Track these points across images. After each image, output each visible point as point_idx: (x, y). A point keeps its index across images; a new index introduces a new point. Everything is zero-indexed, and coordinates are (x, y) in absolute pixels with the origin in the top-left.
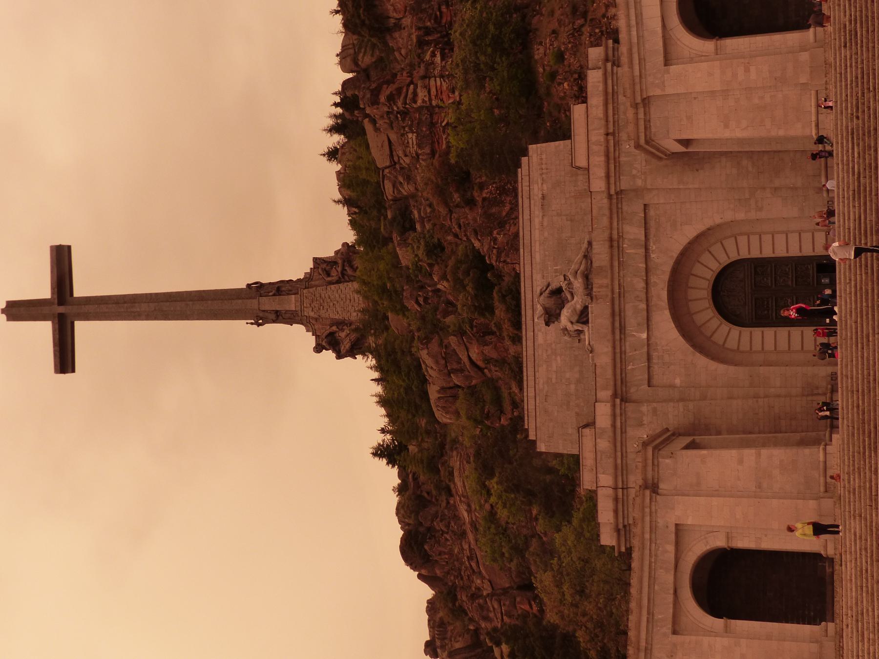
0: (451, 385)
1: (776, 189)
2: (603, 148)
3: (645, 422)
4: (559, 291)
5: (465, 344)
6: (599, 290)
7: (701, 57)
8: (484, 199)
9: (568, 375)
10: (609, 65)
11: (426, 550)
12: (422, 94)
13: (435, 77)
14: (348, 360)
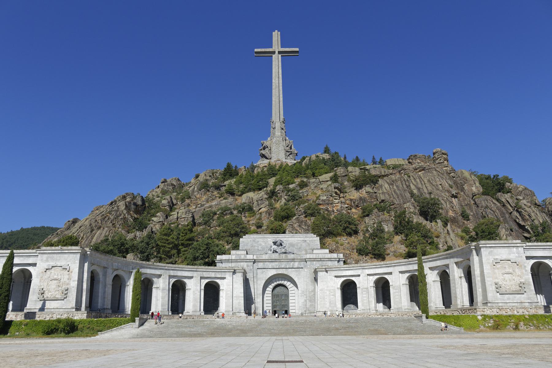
1: (306, 301)
2: (317, 258)
4: (281, 245)
8: (307, 221)
9: (260, 247)
10: (338, 259)
12: (337, 201)
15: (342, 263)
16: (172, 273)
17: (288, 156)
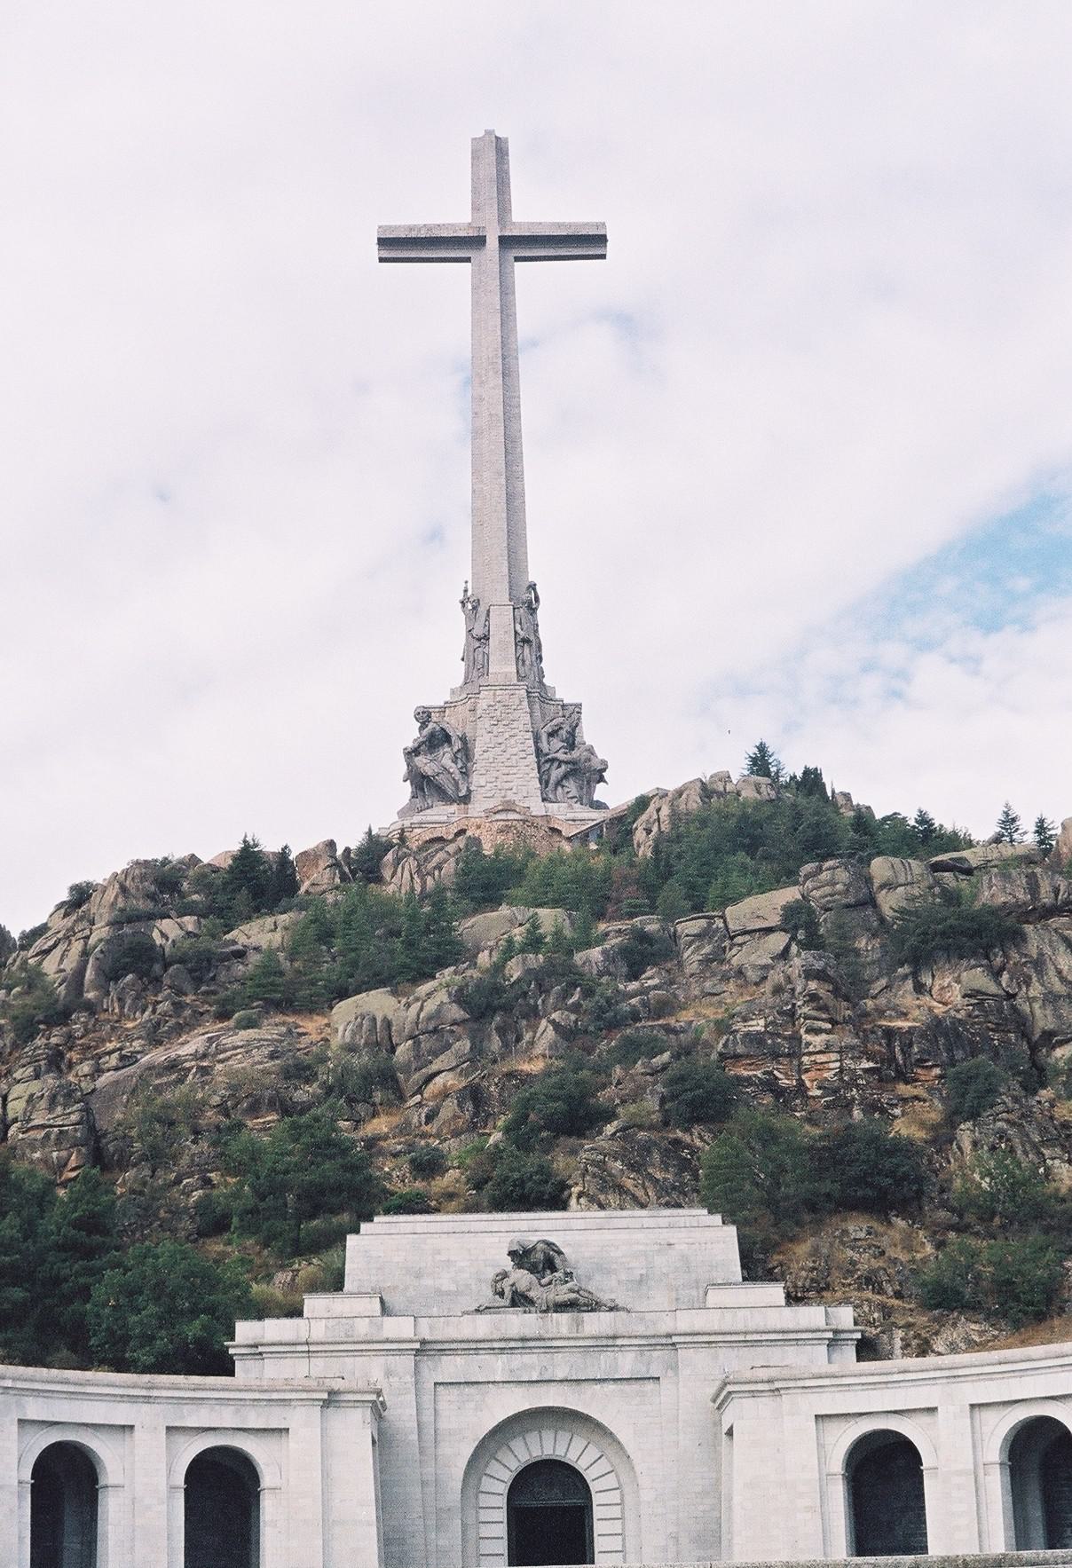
0: (395, 1040)
1: (676, 1539)
3: (391, 1380)
4: (550, 1265)
5: (458, 1066)
6: (554, 1321)
7: (822, 1459)
10: (830, 1335)
12: (818, 1041)
13: (840, 1061)
14: (403, 768)
15: (850, 1352)
16: (35, 1409)
17: (559, 783)
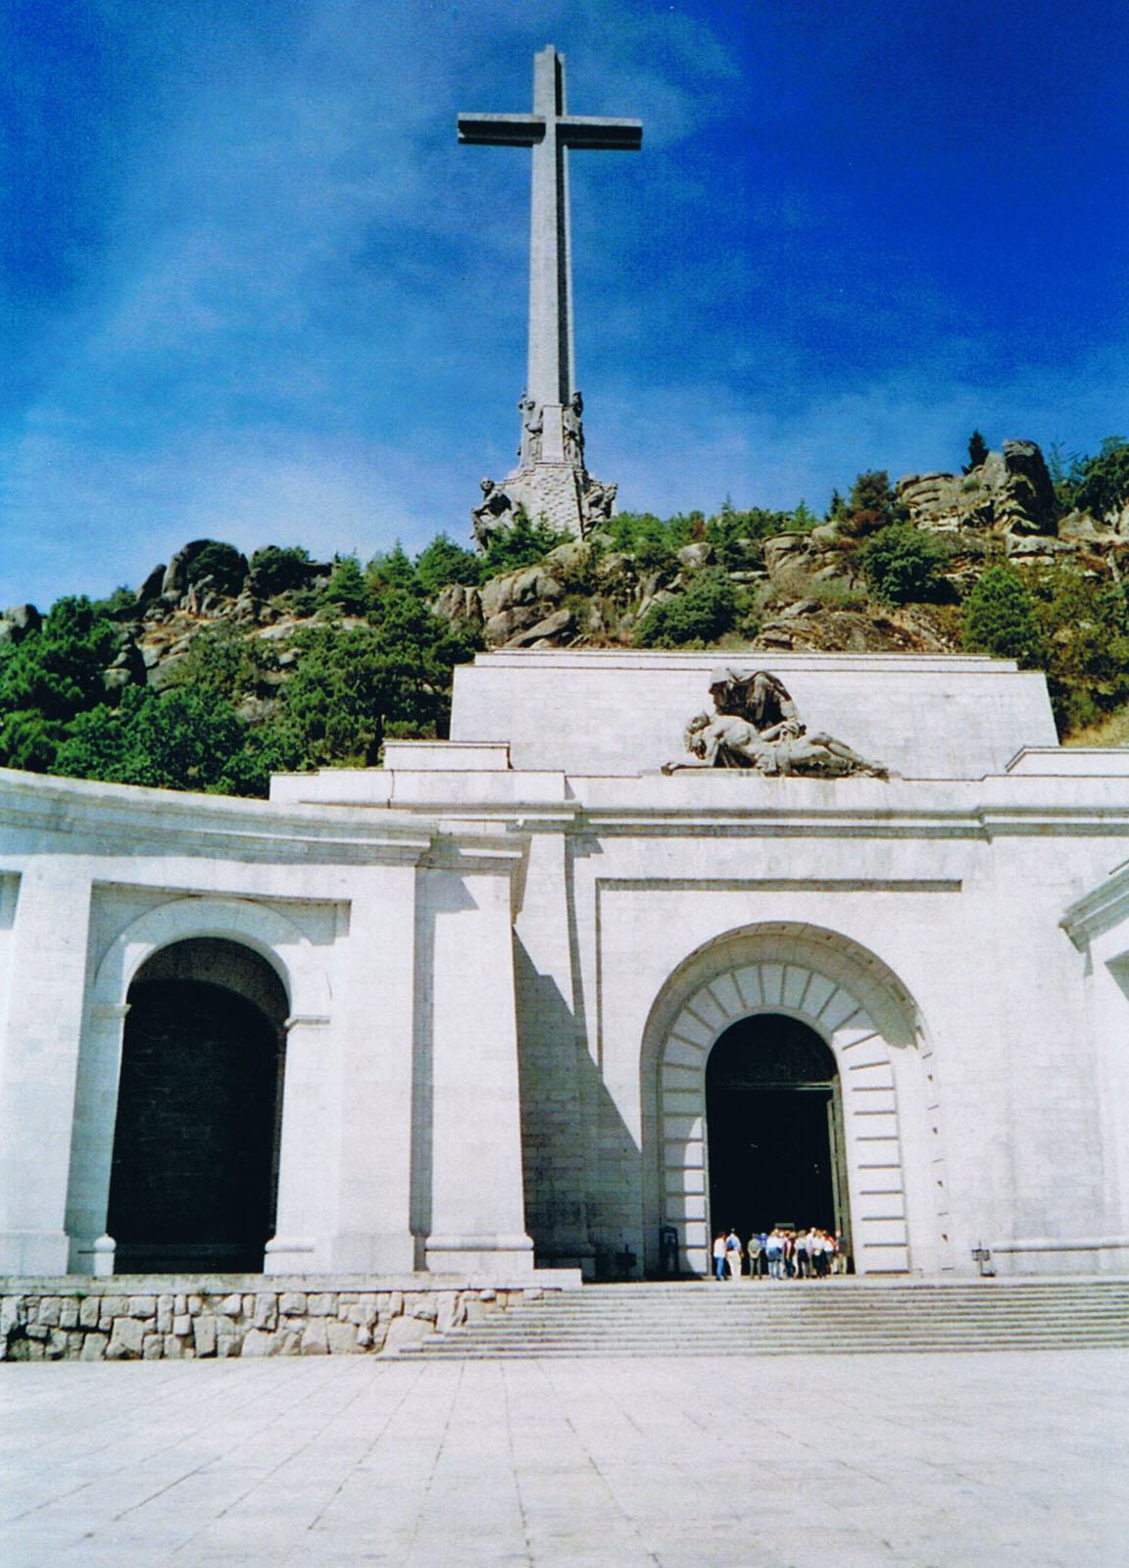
11: (204, 577)
